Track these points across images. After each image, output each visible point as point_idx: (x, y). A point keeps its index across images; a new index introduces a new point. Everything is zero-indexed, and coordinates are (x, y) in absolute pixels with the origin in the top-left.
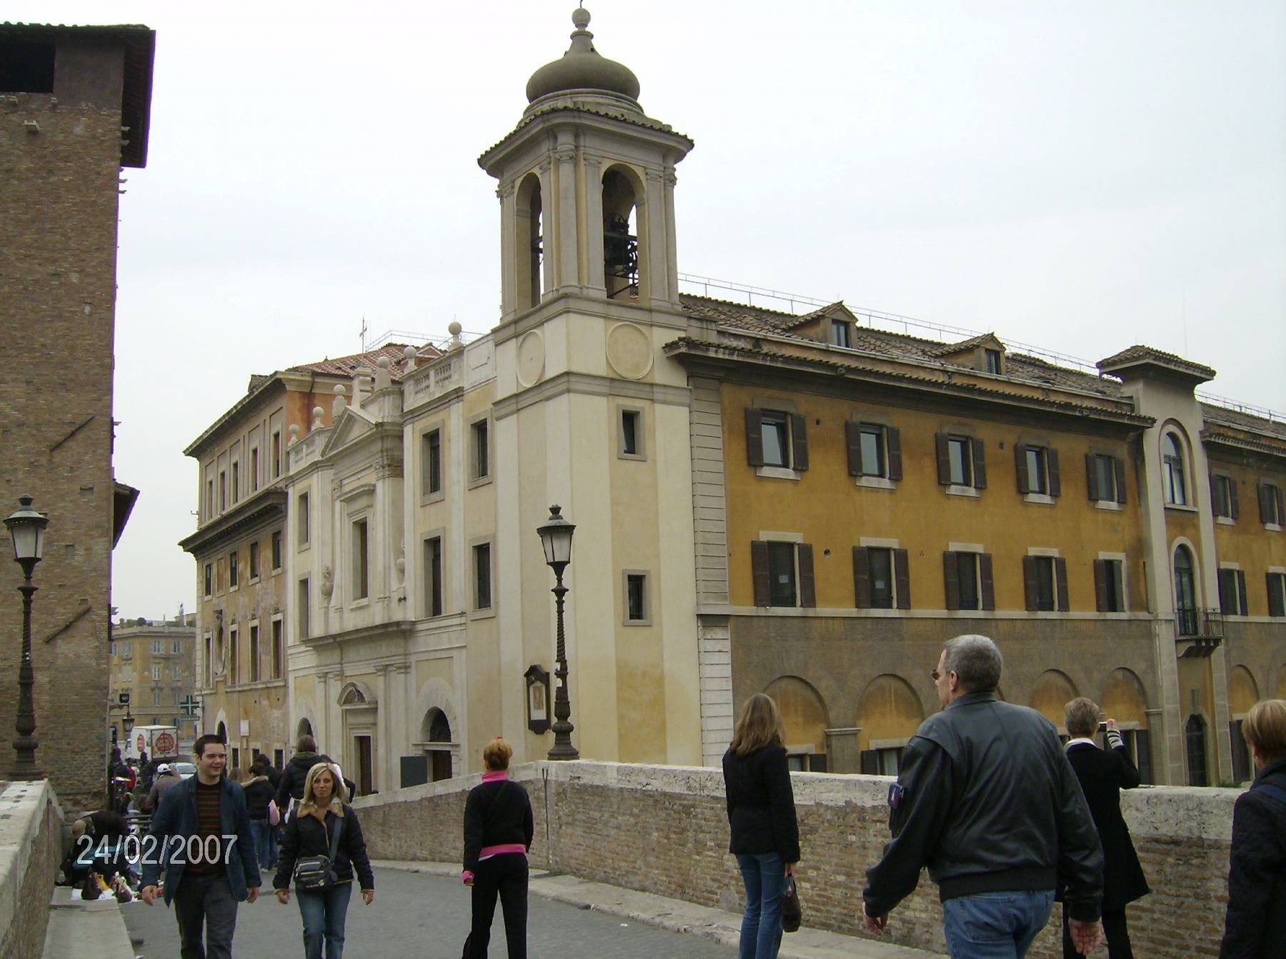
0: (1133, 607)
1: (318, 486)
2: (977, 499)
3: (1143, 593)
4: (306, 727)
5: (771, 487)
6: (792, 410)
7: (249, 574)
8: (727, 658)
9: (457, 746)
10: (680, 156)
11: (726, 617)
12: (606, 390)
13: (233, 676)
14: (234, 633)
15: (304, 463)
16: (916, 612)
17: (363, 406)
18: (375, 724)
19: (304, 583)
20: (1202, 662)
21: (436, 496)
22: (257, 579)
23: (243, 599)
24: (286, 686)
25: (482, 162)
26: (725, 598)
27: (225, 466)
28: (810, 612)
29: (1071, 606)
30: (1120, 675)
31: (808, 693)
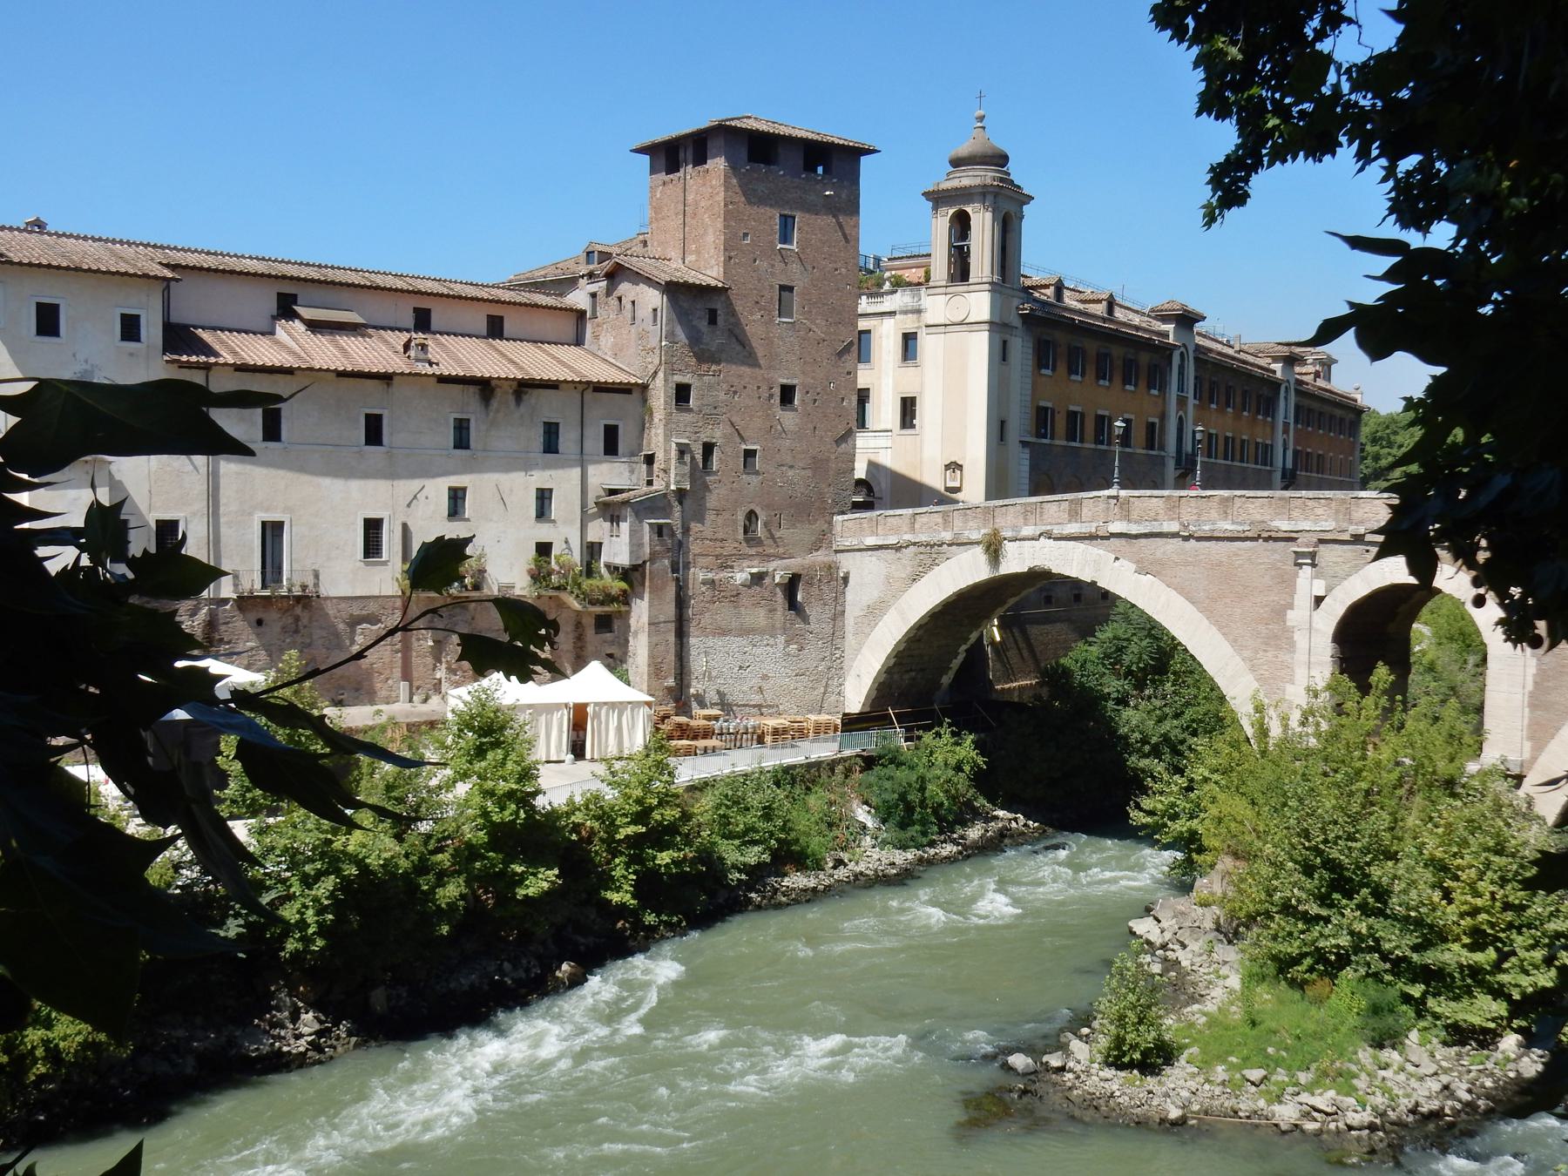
0: (1159, 449)
2: (1108, 388)
8: (1027, 462)
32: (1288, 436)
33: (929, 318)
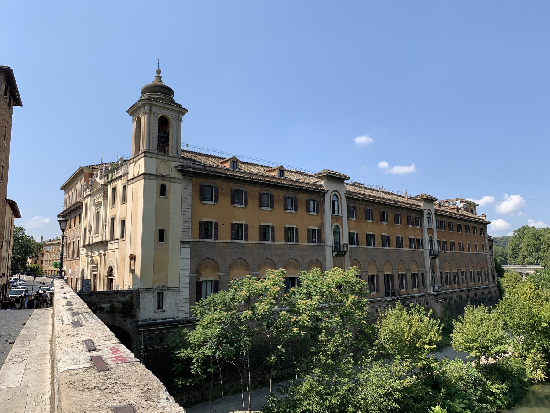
1: (89, 200)
2: (271, 211)
3: (323, 238)
4: (83, 270)
5: (207, 206)
6: (215, 186)
7: (73, 226)
8: (189, 253)
9: (115, 277)
10: (184, 114)
11: (190, 242)
12: (156, 179)
13: (68, 256)
14: (69, 243)
15: (87, 195)
16: (250, 242)
17: (100, 179)
18: (97, 271)
19: (85, 229)
20: (341, 258)
21: (114, 206)
22: (75, 227)
23: (72, 233)
24: (79, 259)
25: (128, 111)
26: (190, 237)
27: (70, 194)
28: (216, 241)
29: (299, 241)
30: (314, 261)
31: (214, 263)
32: (433, 234)
33: (130, 176)
